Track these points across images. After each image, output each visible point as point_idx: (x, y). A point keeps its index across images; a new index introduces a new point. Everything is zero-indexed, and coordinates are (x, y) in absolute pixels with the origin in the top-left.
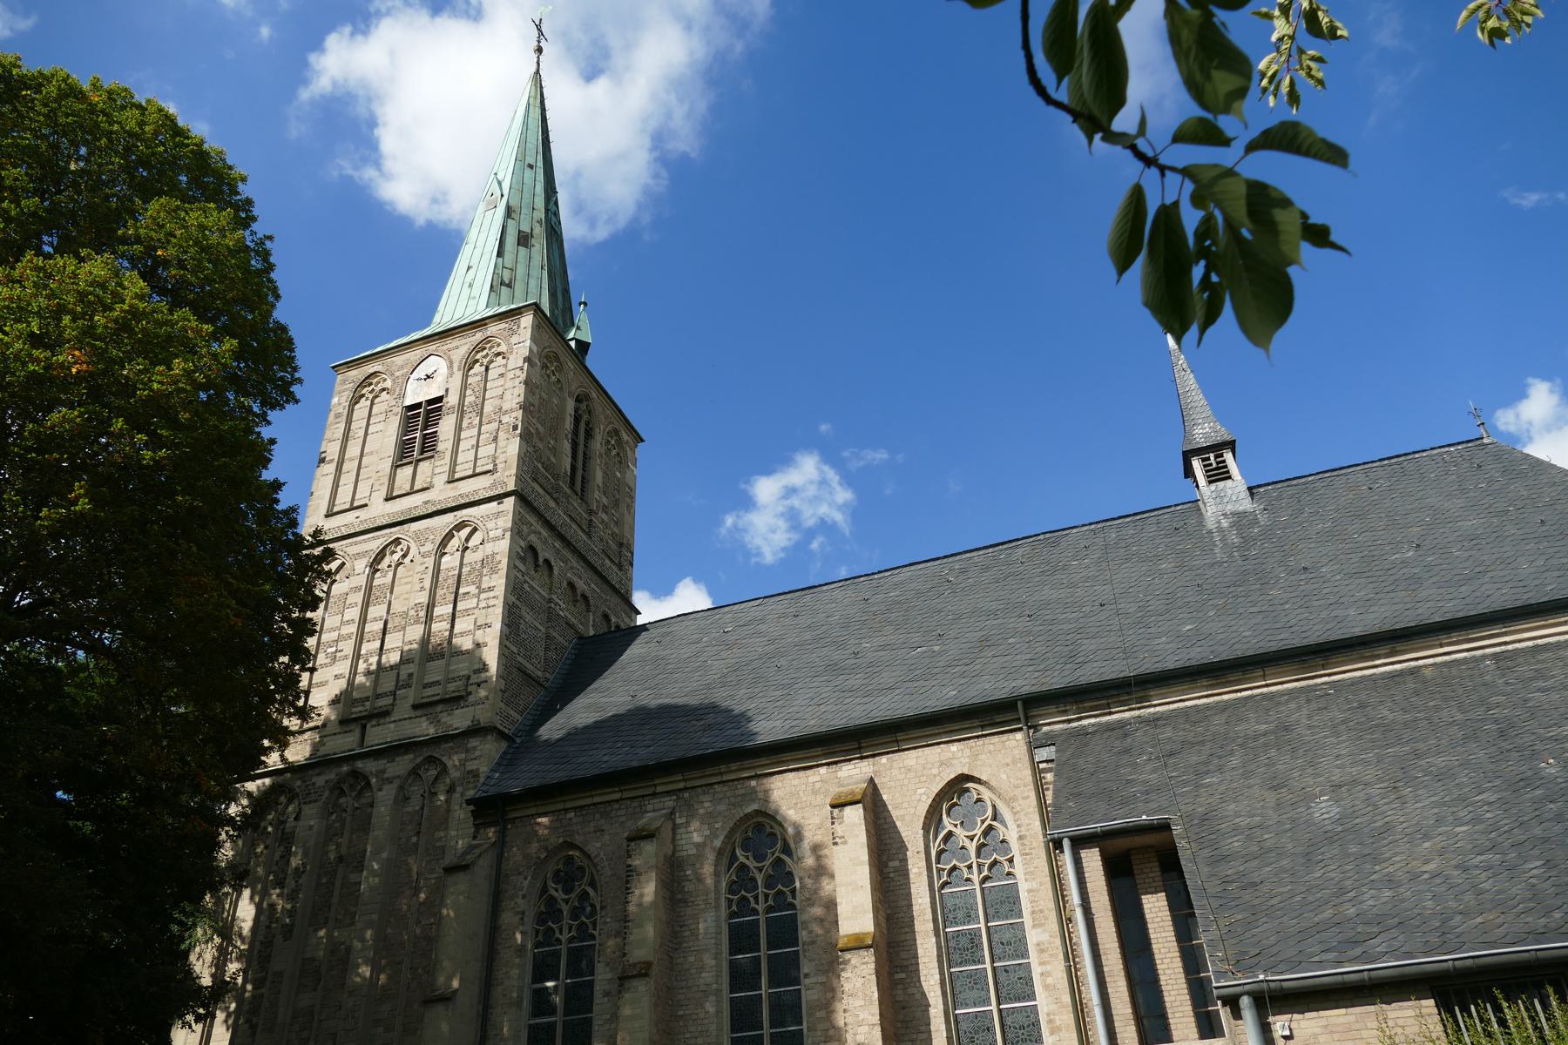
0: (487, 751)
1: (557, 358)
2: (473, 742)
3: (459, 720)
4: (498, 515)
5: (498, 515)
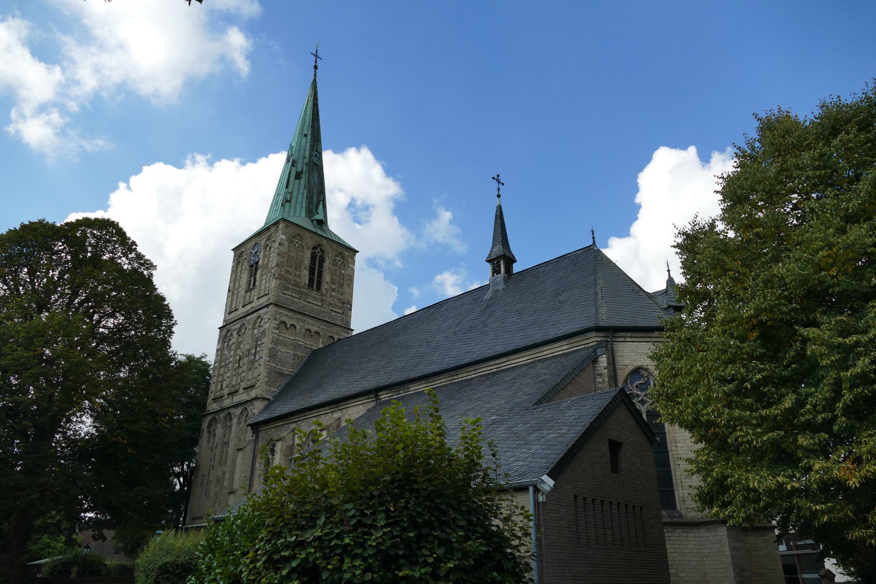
0: (259, 405)
1: (299, 235)
2: (255, 402)
3: (253, 394)
4: (267, 312)
5: (267, 312)
